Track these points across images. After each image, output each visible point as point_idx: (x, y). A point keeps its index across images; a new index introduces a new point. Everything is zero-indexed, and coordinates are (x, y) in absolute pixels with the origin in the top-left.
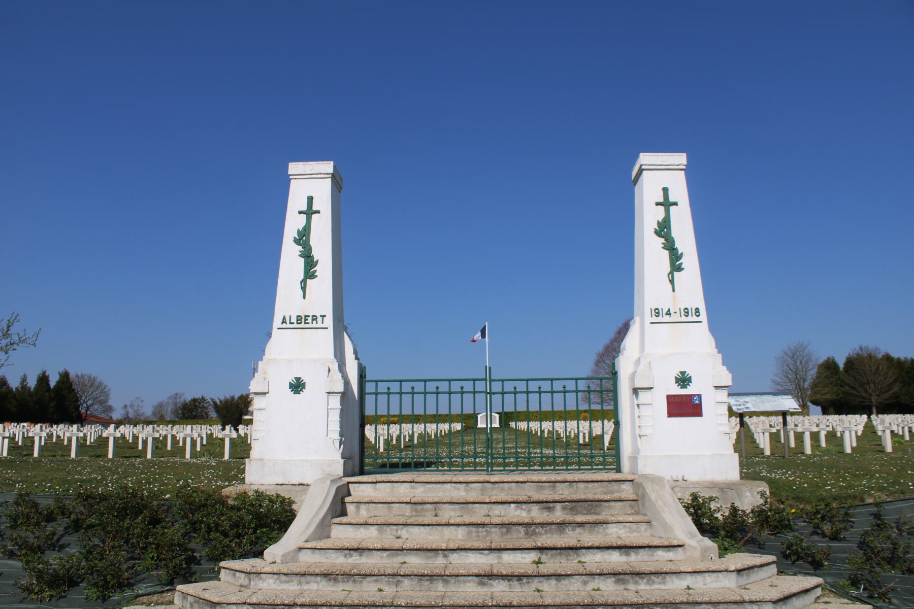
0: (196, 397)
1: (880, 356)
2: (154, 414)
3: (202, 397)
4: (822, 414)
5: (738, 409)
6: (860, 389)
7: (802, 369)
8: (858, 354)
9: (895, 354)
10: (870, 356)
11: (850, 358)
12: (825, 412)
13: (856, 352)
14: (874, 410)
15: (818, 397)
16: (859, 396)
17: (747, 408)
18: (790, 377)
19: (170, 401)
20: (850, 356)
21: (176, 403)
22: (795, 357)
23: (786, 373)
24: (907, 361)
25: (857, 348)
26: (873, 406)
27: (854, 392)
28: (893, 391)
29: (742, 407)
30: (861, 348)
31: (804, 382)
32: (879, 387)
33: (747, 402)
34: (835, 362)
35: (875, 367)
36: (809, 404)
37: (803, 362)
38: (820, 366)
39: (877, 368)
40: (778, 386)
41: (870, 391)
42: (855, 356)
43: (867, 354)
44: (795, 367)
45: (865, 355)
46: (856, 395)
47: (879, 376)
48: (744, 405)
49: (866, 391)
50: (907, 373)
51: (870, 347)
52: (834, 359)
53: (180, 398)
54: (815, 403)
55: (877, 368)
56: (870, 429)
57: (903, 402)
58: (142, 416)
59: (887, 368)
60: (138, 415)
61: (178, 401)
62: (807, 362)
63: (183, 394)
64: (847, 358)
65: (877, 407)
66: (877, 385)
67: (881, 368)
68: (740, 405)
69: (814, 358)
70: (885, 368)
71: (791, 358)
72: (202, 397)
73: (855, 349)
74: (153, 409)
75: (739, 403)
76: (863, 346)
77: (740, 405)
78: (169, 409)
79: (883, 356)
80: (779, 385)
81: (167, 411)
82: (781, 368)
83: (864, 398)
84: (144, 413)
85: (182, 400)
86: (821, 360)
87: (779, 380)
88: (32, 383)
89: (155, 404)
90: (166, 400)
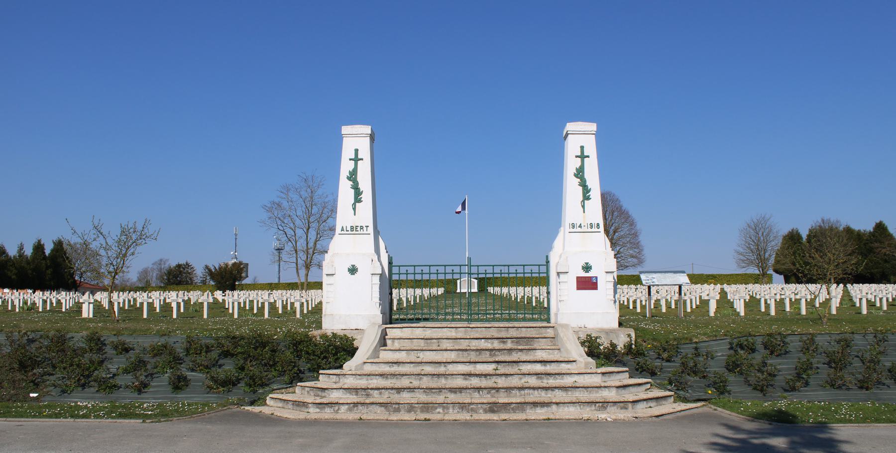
0: (180, 263)
1: (841, 228)
2: (139, 280)
3: (187, 263)
4: (784, 282)
5: (646, 283)
7: (764, 240)
12: (787, 281)
13: (818, 224)
14: (832, 281)
15: (778, 267)
17: (653, 282)
18: (752, 247)
19: (155, 267)
20: (813, 228)
21: (161, 269)
22: (757, 228)
23: (749, 244)
24: (866, 234)
25: (820, 220)
29: (650, 281)
30: (823, 221)
31: (765, 253)
33: (654, 278)
34: (799, 233)
37: (765, 234)
38: (785, 238)
40: (741, 256)
42: (818, 228)
43: (829, 226)
44: (757, 238)
45: (827, 227)
48: (651, 280)
50: (865, 244)
51: (832, 220)
52: (798, 231)
53: (165, 264)
56: (847, 296)
58: (128, 281)
59: (847, 240)
60: (124, 281)
61: (162, 267)
62: (768, 235)
63: (167, 260)
68: (648, 280)
69: (775, 231)
71: (753, 230)
72: (187, 263)
73: (818, 222)
74: (138, 275)
75: (648, 278)
76: (825, 219)
77: (648, 280)
78: (155, 275)
79: (844, 228)
80: (742, 255)
81: (152, 276)
82: (744, 239)
84: (129, 279)
85: (167, 265)
86: (785, 230)
87: (742, 250)
88: (29, 251)
89: (141, 270)
90: (151, 266)
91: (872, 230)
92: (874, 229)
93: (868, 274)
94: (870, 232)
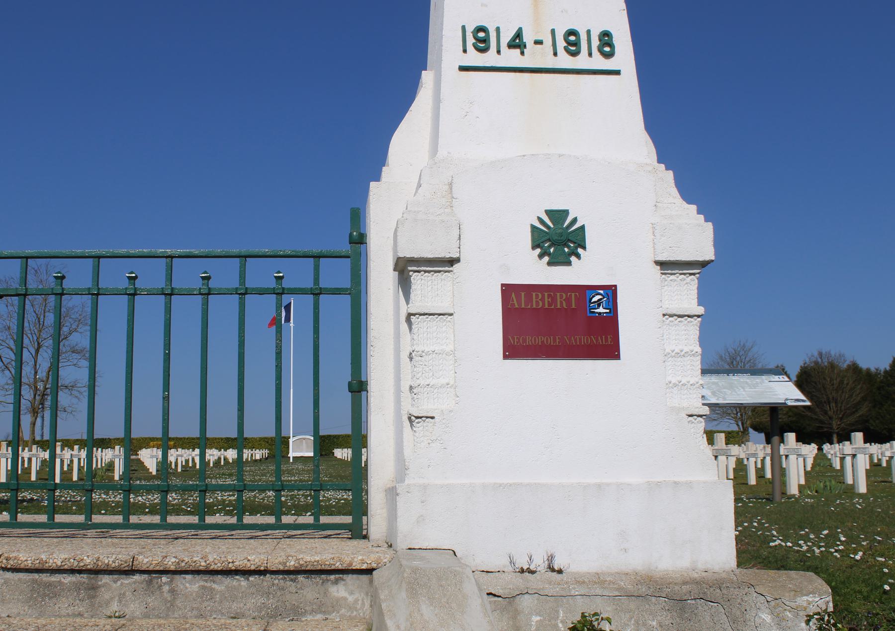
1: (845, 366)
6: (817, 410)
8: (816, 363)
9: (864, 365)
10: (832, 366)
11: (806, 368)
13: (814, 359)
14: (835, 439)
16: (817, 419)
20: (806, 365)
22: (735, 363)
25: (816, 354)
26: (834, 433)
27: (809, 414)
28: (860, 413)
30: (820, 354)
32: (843, 407)
35: (838, 380)
36: (751, 430)
39: (841, 382)
41: (830, 413)
43: (829, 363)
45: (826, 364)
46: (812, 418)
47: (843, 392)
49: (826, 413)
50: (879, 388)
51: (833, 353)
54: (757, 428)
55: (841, 382)
57: (872, 428)
59: (854, 382)
64: (801, 367)
65: (838, 434)
66: (839, 405)
67: (845, 382)
70: (850, 383)
73: (813, 356)
76: (824, 352)
79: (849, 366)
83: (822, 422)
91: (888, 368)
92: (891, 366)
93: (885, 432)
94: (886, 372)
